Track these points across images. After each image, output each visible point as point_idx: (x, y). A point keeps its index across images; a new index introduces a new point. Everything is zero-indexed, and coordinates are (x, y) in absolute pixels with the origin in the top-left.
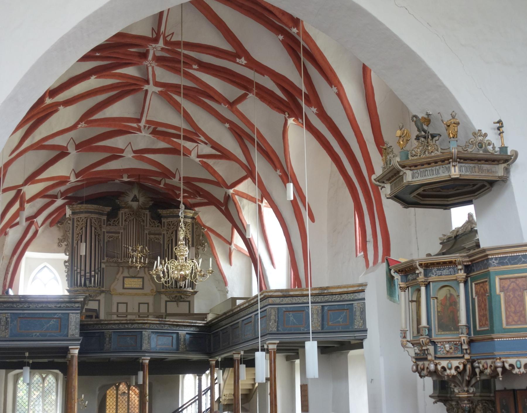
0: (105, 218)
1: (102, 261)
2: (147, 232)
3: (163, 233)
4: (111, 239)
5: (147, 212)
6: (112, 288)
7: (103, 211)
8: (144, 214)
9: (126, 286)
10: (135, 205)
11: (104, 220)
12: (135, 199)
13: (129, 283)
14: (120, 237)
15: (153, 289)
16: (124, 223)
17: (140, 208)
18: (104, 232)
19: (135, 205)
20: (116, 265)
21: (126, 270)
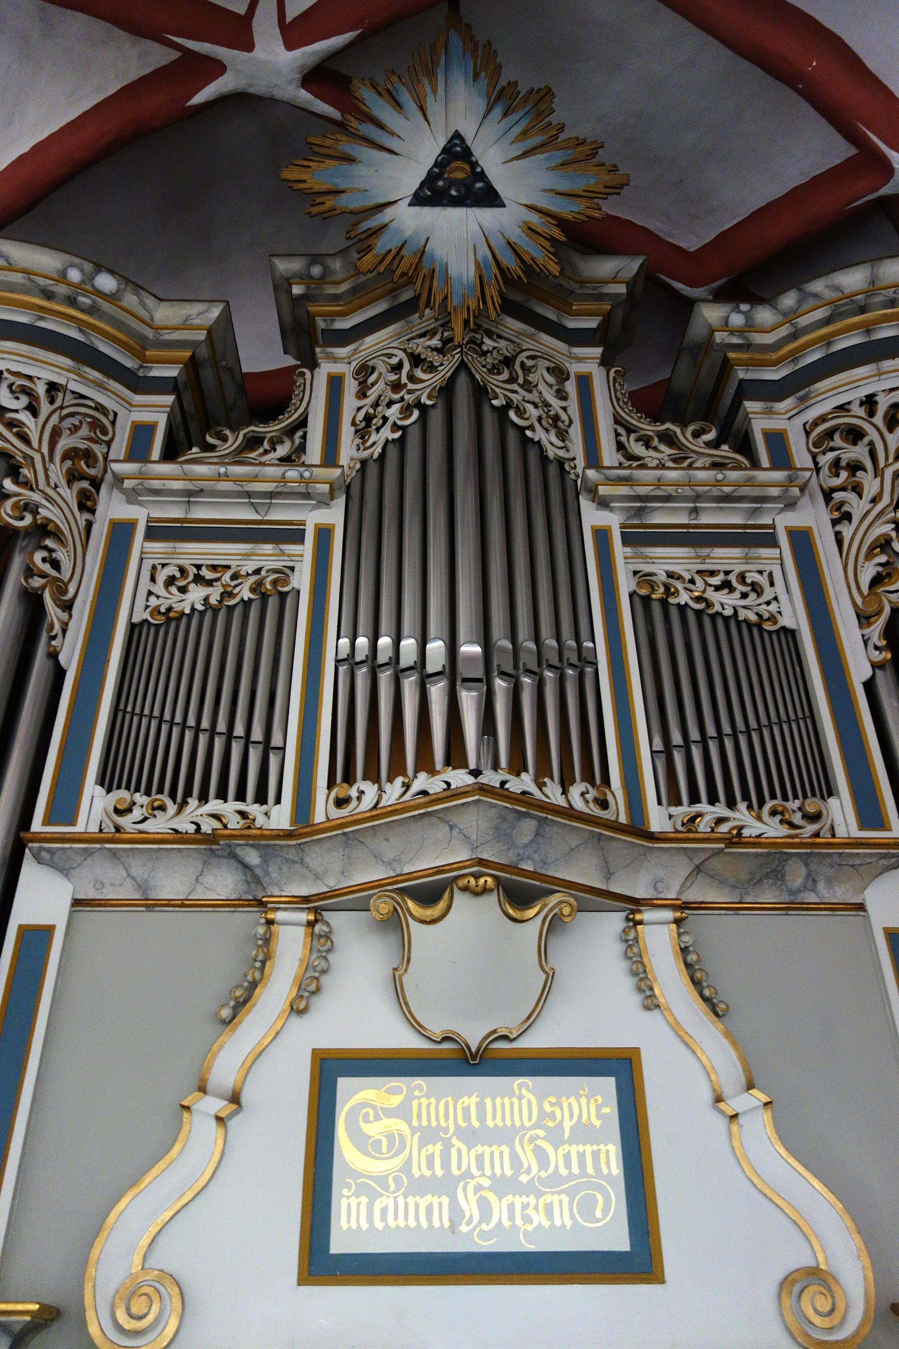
0: (155, 410)
1: (37, 825)
2: (613, 520)
3: (784, 521)
4: (196, 595)
5: (587, 360)
6: (114, 1261)
7: (139, 346)
8: (560, 373)
9: (355, 1225)
10: (456, 238)
11: (142, 434)
12: (456, 182)
13: (411, 1161)
14: (302, 580)
15: (814, 1276)
16: (348, 450)
17: (520, 289)
18: (121, 532)
19: (456, 238)
20: (223, 883)
21: (360, 956)
